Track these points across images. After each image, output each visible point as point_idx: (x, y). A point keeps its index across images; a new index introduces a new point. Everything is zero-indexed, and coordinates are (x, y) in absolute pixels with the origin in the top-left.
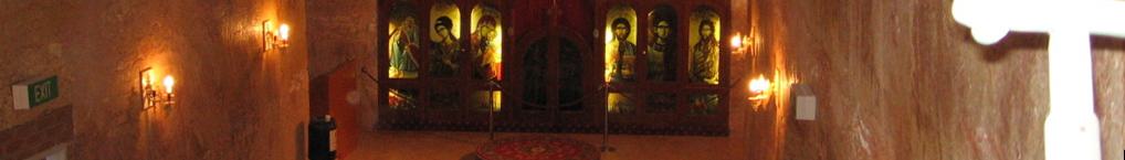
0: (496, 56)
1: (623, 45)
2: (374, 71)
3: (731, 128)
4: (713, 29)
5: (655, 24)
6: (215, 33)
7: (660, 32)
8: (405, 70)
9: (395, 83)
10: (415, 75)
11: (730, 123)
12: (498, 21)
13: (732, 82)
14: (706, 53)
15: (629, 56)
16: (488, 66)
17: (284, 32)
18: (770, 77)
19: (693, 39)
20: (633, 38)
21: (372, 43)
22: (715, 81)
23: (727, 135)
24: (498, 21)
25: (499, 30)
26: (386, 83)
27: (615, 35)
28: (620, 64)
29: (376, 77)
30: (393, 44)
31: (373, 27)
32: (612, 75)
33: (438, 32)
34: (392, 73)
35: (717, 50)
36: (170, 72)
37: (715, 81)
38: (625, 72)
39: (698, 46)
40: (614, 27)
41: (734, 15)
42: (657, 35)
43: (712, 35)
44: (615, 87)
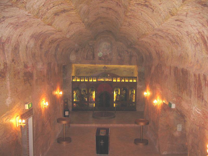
0: (94, 97)
1: (117, 93)
2: (71, 100)
3: (137, 109)
4: (134, 92)
5: (123, 91)
6: (51, 94)
7: (124, 92)
8: (77, 100)
9: (75, 102)
10: (79, 101)
11: (137, 108)
12: (94, 90)
13: (137, 101)
14: (133, 96)
15: (118, 97)
16: (92, 99)
17: (61, 93)
18: (157, 100)
19: (130, 93)
20: (119, 93)
21: (71, 95)
22: (134, 101)
23: (136, 111)
24: (94, 90)
25: (94, 92)
26: (73, 102)
27: (116, 93)
28: (117, 97)
29: (71, 101)
30: (75, 95)
31: (71, 92)
32: (115, 100)
33: (83, 93)
34: (74, 100)
35: (134, 95)
36: (48, 101)
37: (134, 101)
38: (118, 100)
39: (131, 95)
40: (116, 91)
41: (137, 89)
42: (123, 93)
43: (133, 93)
44: (115, 102)
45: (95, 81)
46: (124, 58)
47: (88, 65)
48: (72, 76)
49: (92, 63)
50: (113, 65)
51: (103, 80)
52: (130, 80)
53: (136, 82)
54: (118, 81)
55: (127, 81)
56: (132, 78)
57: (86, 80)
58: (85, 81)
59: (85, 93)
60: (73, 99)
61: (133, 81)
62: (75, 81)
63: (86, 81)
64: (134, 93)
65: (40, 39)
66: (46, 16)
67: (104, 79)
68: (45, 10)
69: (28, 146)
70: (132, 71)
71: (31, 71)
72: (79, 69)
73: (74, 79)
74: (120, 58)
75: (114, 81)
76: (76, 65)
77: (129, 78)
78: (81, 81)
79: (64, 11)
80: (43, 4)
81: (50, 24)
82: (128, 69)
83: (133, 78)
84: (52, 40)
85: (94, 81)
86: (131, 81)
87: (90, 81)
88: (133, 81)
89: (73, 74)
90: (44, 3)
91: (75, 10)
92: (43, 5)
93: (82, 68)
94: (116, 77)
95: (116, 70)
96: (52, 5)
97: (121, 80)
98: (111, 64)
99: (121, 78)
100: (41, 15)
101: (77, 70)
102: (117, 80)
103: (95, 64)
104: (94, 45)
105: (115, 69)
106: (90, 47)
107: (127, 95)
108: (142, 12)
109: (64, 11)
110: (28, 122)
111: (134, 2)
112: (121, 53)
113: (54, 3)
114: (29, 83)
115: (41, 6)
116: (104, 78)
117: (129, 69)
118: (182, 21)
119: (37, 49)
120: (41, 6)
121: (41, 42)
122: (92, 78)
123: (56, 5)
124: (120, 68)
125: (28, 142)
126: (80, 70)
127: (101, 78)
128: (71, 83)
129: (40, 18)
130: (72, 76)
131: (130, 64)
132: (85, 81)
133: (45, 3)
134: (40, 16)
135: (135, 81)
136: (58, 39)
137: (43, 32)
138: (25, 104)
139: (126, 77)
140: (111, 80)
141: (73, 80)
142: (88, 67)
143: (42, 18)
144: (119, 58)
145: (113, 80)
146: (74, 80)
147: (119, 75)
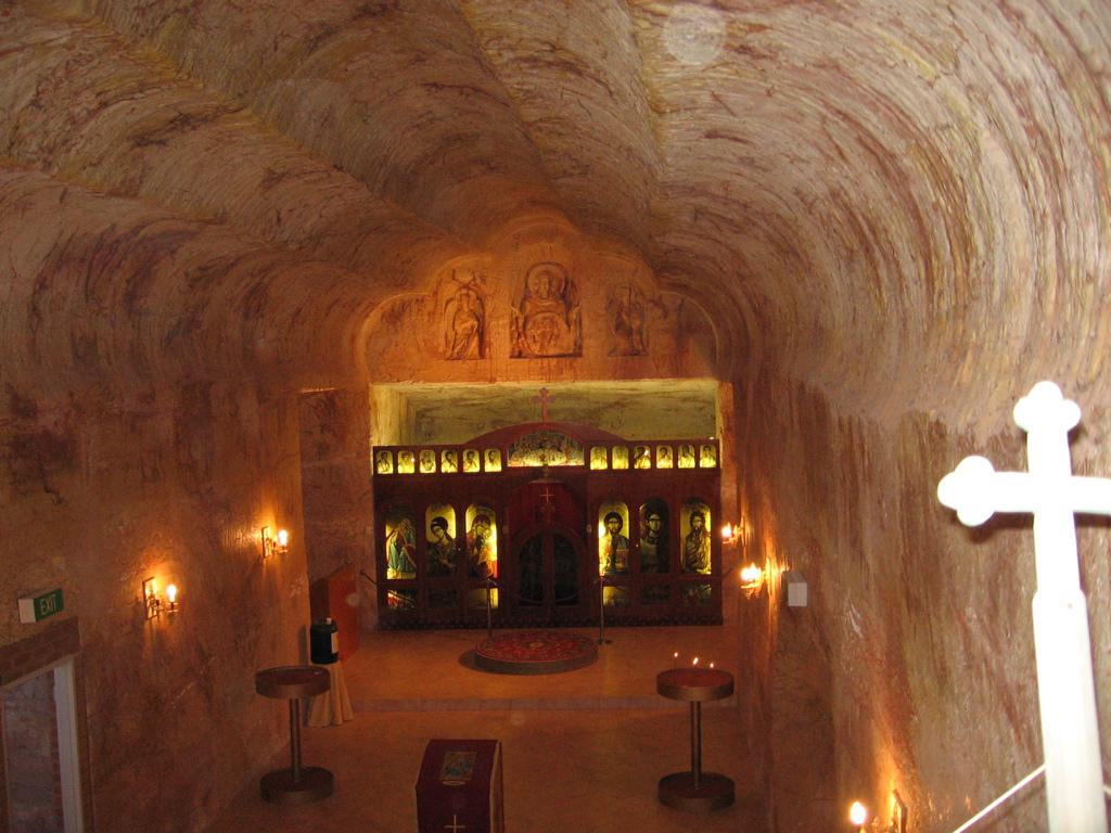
0: (493, 555)
1: (616, 535)
2: (373, 573)
3: (725, 617)
4: (703, 521)
5: (647, 517)
6: (214, 538)
7: (652, 525)
8: (403, 571)
9: (393, 584)
10: (414, 576)
11: (724, 612)
12: (493, 519)
13: (724, 572)
14: (698, 544)
15: (622, 550)
16: (484, 564)
17: (283, 537)
18: (761, 565)
19: (685, 531)
20: (626, 531)
21: (370, 547)
22: (707, 571)
23: (721, 623)
24: (493, 519)
25: (494, 528)
26: (385, 585)
27: (608, 529)
28: (613, 557)
29: (375, 579)
30: (390, 545)
31: (370, 530)
32: (606, 568)
33: (434, 532)
34: (391, 574)
35: (709, 540)
36: (173, 581)
37: (707, 571)
38: (619, 565)
39: (690, 537)
40: (607, 522)
41: (724, 505)
42: (649, 529)
43: (703, 526)
44: (609, 581)
45: (493, 467)
46: (648, 342)
47: (463, 385)
48: (372, 445)
49: (474, 376)
50: (584, 379)
51: (533, 462)
52: (683, 459)
53: (715, 471)
54: (620, 463)
55: (664, 463)
56: (692, 450)
57: (447, 468)
58: (443, 470)
59: (446, 534)
60: (382, 565)
61: (697, 460)
62: (391, 471)
63: (446, 473)
64: (708, 526)
65: (118, 266)
66: (73, 152)
67: (542, 459)
68: (55, 125)
69: (59, 813)
70: (702, 404)
71: (60, 432)
72: (426, 410)
73: (386, 462)
74: (623, 341)
75: (598, 464)
76: (408, 387)
77: (676, 447)
78: (423, 470)
79: (183, 122)
80: (30, 95)
81: (129, 190)
82: (685, 400)
83: (697, 446)
84: (200, 269)
85: (489, 468)
86: (687, 463)
87: (470, 471)
88: (697, 460)
89: (382, 436)
90: (34, 92)
91: (247, 112)
92: (34, 103)
93: (442, 401)
94: (609, 444)
95: (623, 406)
96: (89, 99)
97: (632, 461)
98: (575, 379)
99: (633, 449)
100: (41, 149)
101: (421, 415)
102: (610, 462)
103: (492, 380)
104: (483, 280)
105: (617, 403)
106: (464, 291)
107: (667, 535)
108: (582, 102)
109: (183, 122)
110: (56, 688)
111: (504, 53)
112: (628, 315)
113: (98, 89)
114: (47, 491)
115: (17, 109)
116: (541, 452)
117: (694, 399)
118: (740, 137)
119: (105, 316)
120: (17, 109)
121: (128, 281)
122: (477, 454)
123: (118, 98)
124: (638, 395)
125: (58, 791)
126: (435, 413)
127: (528, 449)
128: (369, 487)
129: (39, 164)
130: (376, 450)
131: (679, 372)
132: (443, 470)
133: (38, 93)
134: (35, 157)
135: (707, 462)
136: (238, 259)
137: (120, 232)
138: (21, 598)
139: (660, 442)
140: (581, 463)
141: (381, 470)
142: (466, 396)
143: (48, 165)
144: (623, 344)
145: (588, 461)
146: (385, 469)
147: (627, 434)
